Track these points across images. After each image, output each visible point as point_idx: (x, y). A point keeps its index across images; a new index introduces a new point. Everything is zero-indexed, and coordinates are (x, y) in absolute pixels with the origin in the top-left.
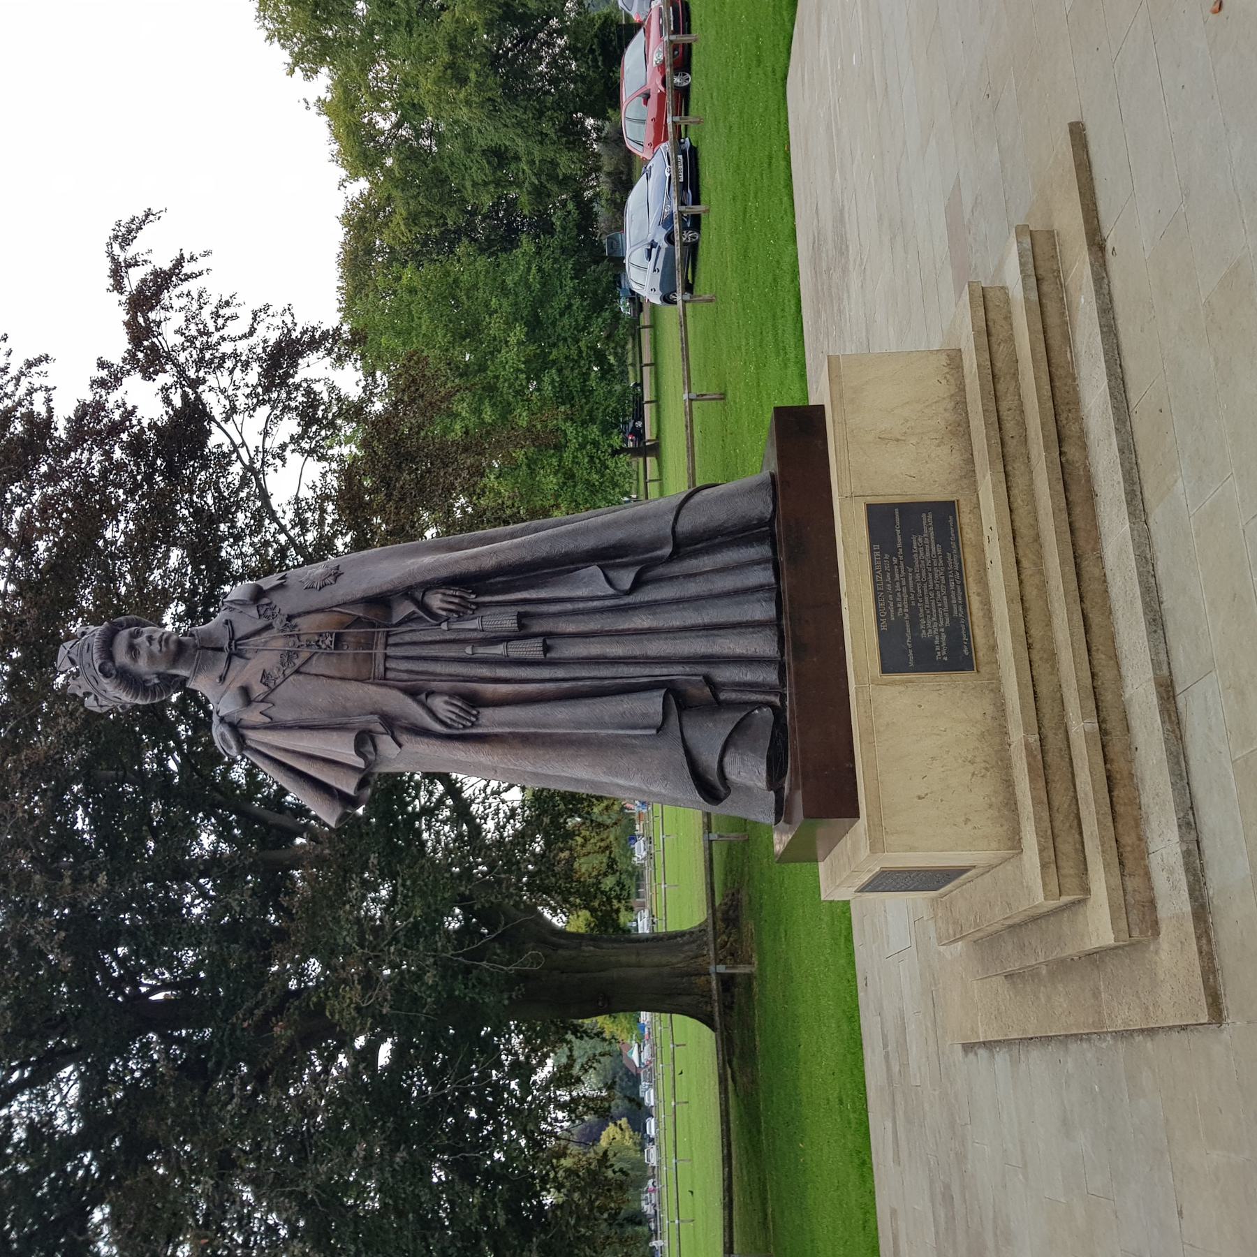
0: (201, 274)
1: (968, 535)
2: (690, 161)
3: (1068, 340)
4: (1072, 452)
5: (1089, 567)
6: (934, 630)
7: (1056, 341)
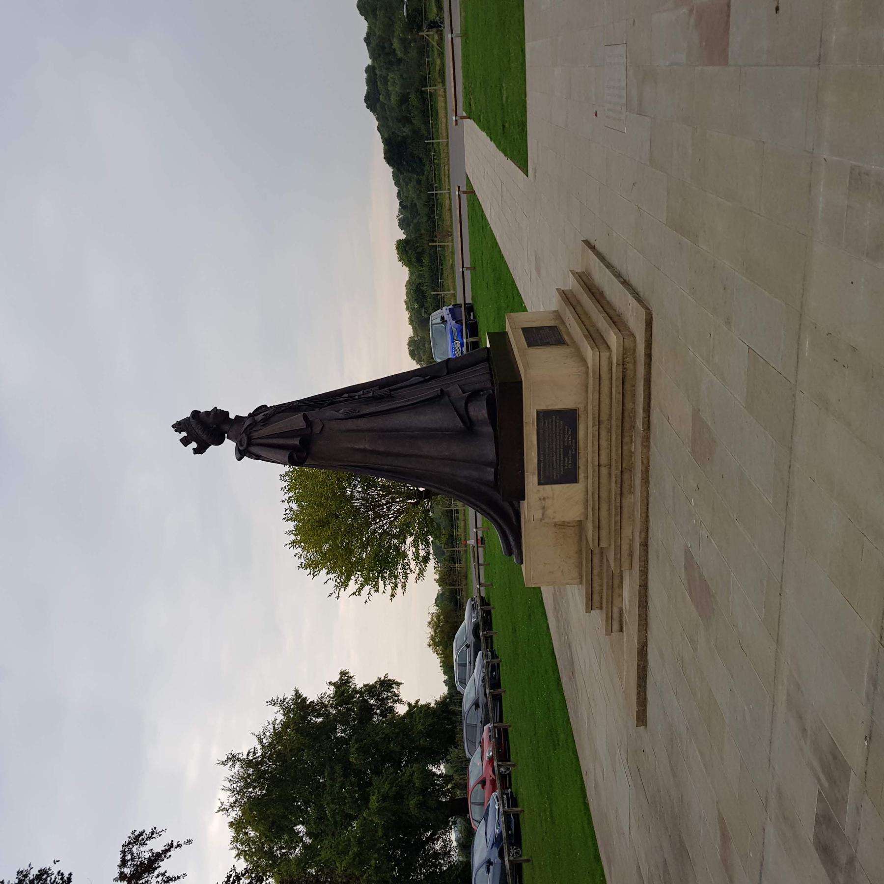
0: (179, 878)
2: (513, 801)
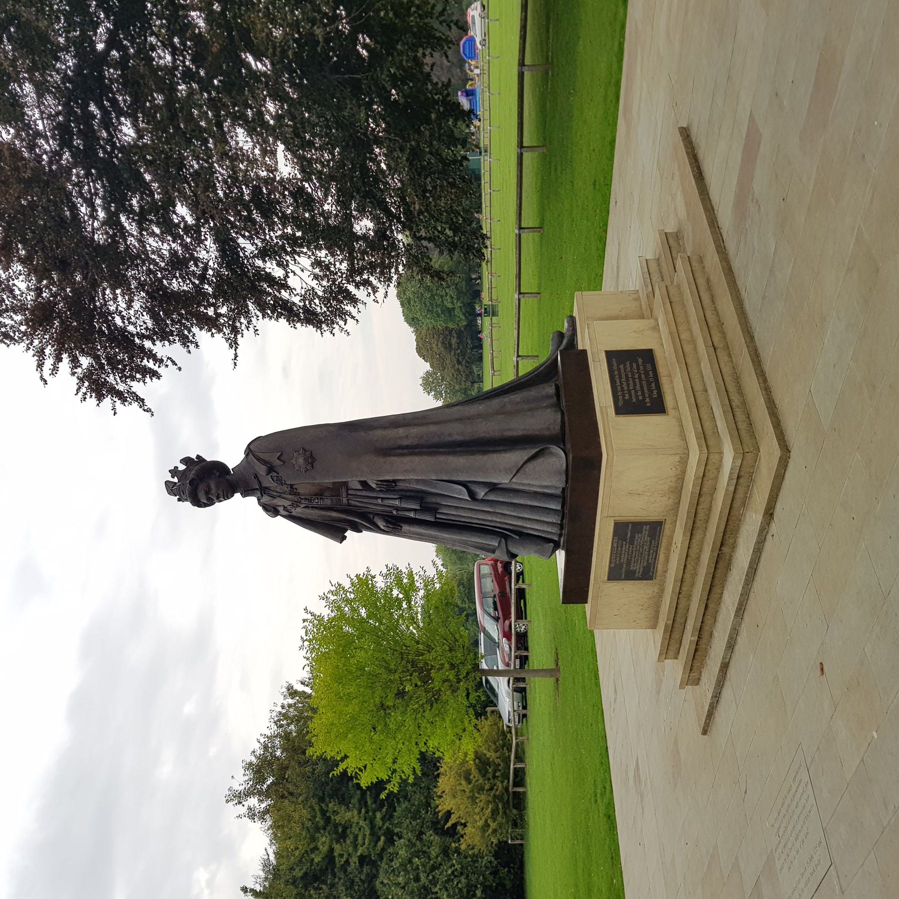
1: (664, 541)
3: (744, 504)
4: (726, 549)
5: (716, 590)
6: (638, 567)
7: (737, 504)
